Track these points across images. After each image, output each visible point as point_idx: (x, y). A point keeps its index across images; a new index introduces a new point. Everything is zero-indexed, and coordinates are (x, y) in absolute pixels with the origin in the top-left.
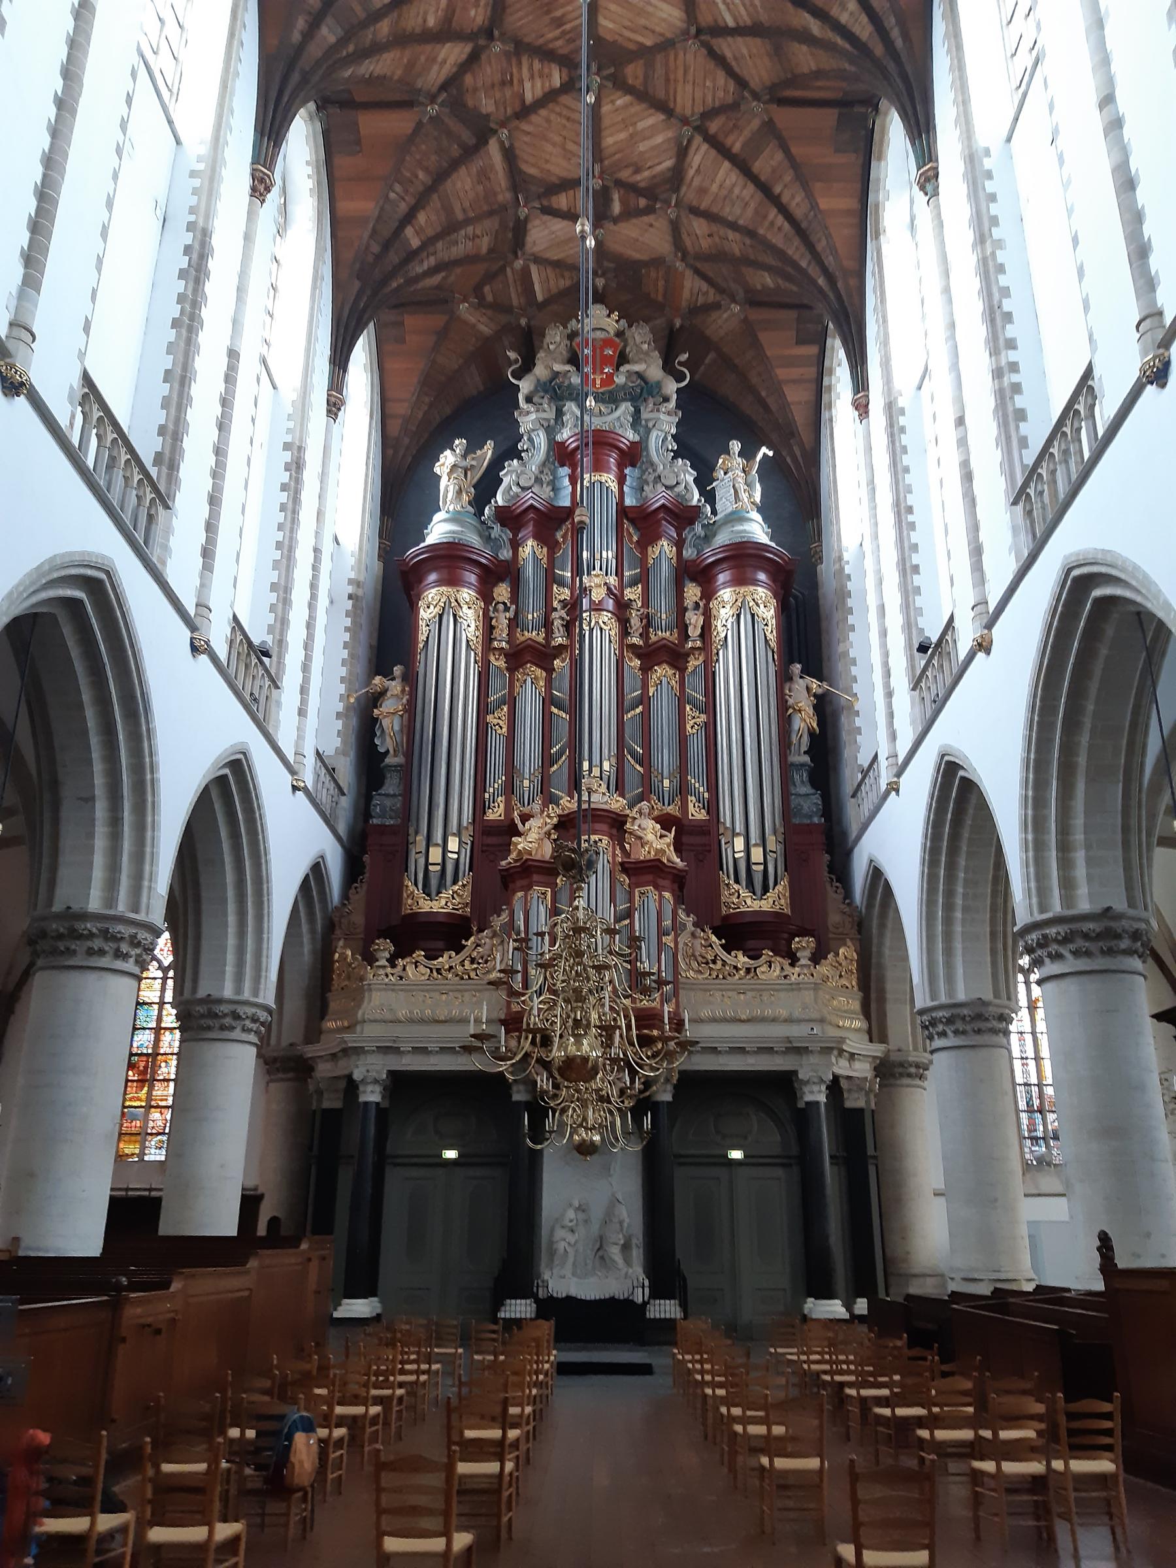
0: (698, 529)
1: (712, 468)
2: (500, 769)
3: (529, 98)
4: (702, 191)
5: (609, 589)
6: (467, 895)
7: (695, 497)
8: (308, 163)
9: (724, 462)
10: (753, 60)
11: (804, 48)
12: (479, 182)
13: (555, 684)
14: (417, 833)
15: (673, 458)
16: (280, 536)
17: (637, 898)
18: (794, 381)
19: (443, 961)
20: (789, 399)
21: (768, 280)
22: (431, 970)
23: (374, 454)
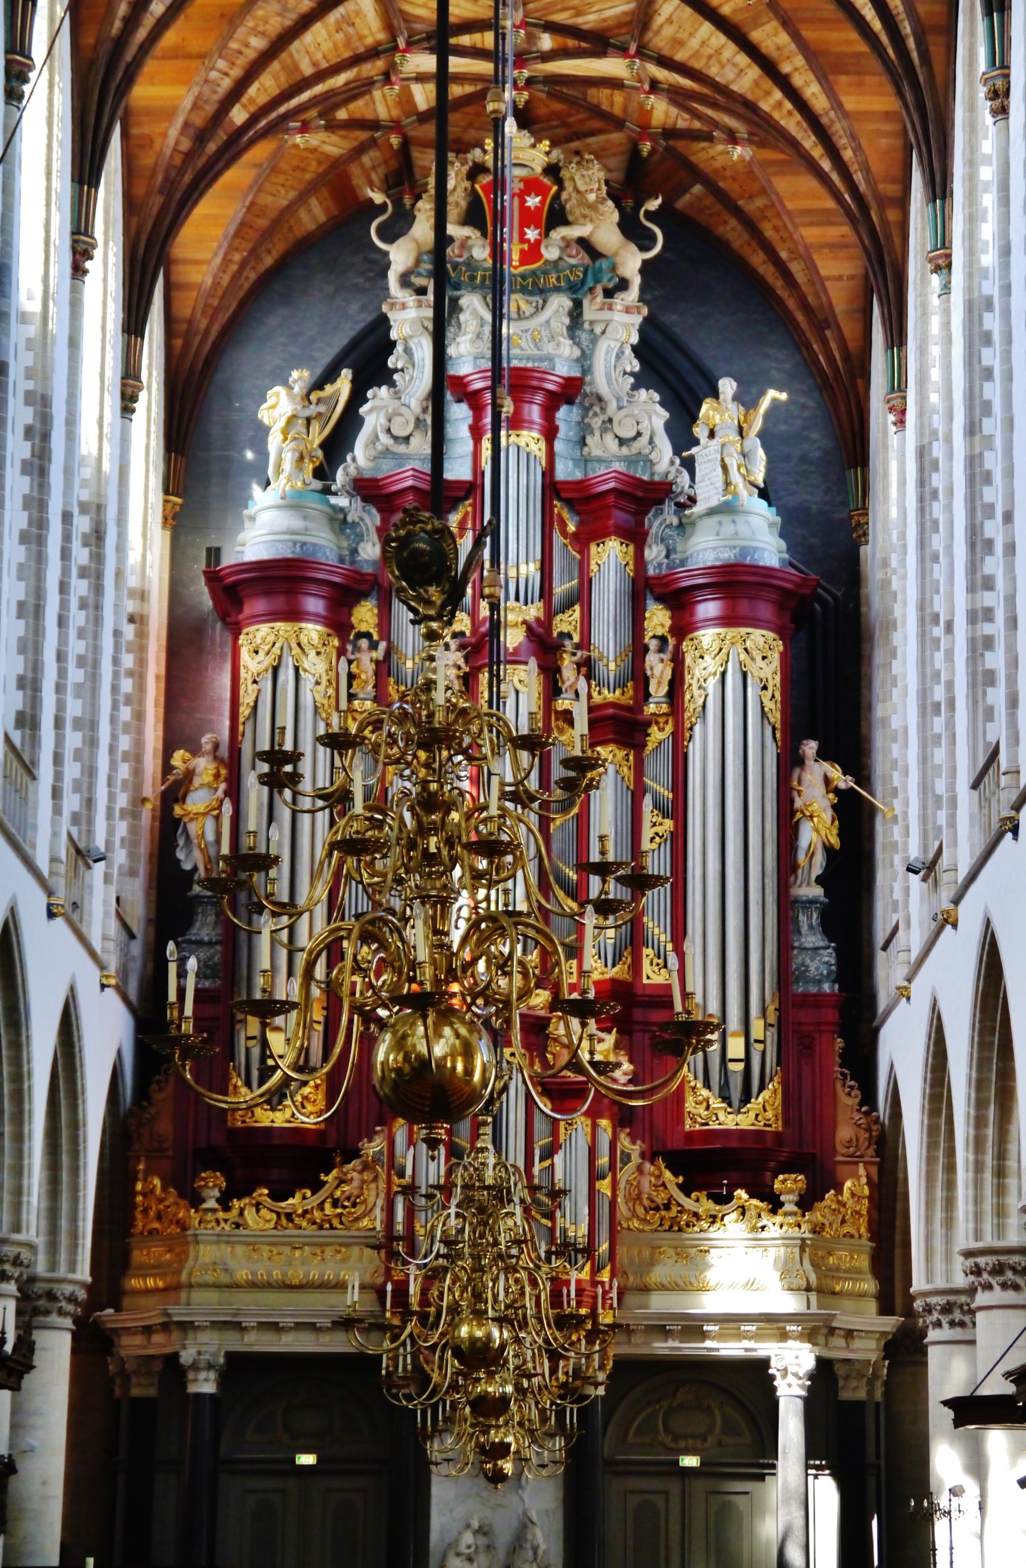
0: (669, 508)
1: (694, 418)
7: (664, 457)
15: (635, 387)
17: (562, 1130)
18: (831, 246)
19: (294, 1202)
20: (823, 272)
22: (278, 1214)
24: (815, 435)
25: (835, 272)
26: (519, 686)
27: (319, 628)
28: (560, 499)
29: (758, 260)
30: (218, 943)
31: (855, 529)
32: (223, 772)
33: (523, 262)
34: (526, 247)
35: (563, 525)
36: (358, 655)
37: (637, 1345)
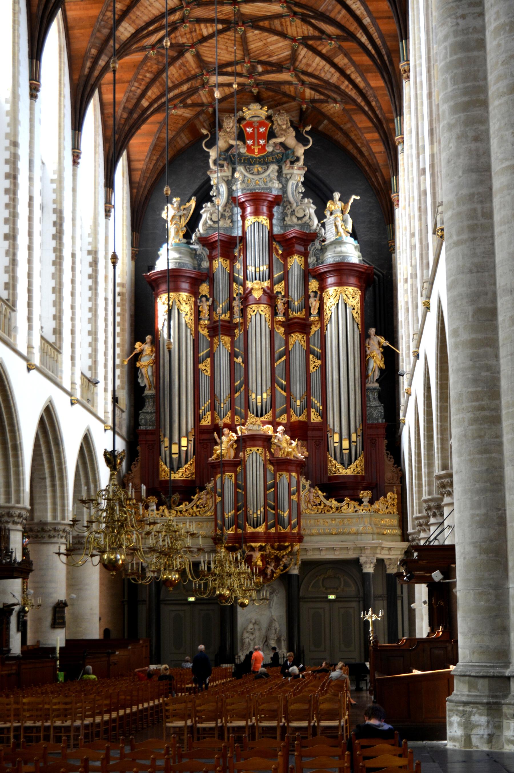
2: (207, 396)
5: (264, 291)
6: (193, 469)
13: (237, 344)
14: (165, 436)
15: (303, 198)
20: (374, 151)
22: (177, 511)
23: (127, 199)
24: (374, 213)
25: (378, 150)
26: (261, 313)
27: (187, 294)
28: (276, 241)
29: (350, 147)
30: (154, 412)
31: (390, 248)
32: (154, 349)
33: (259, 153)
34: (260, 147)
35: (277, 251)
37: (310, 556)
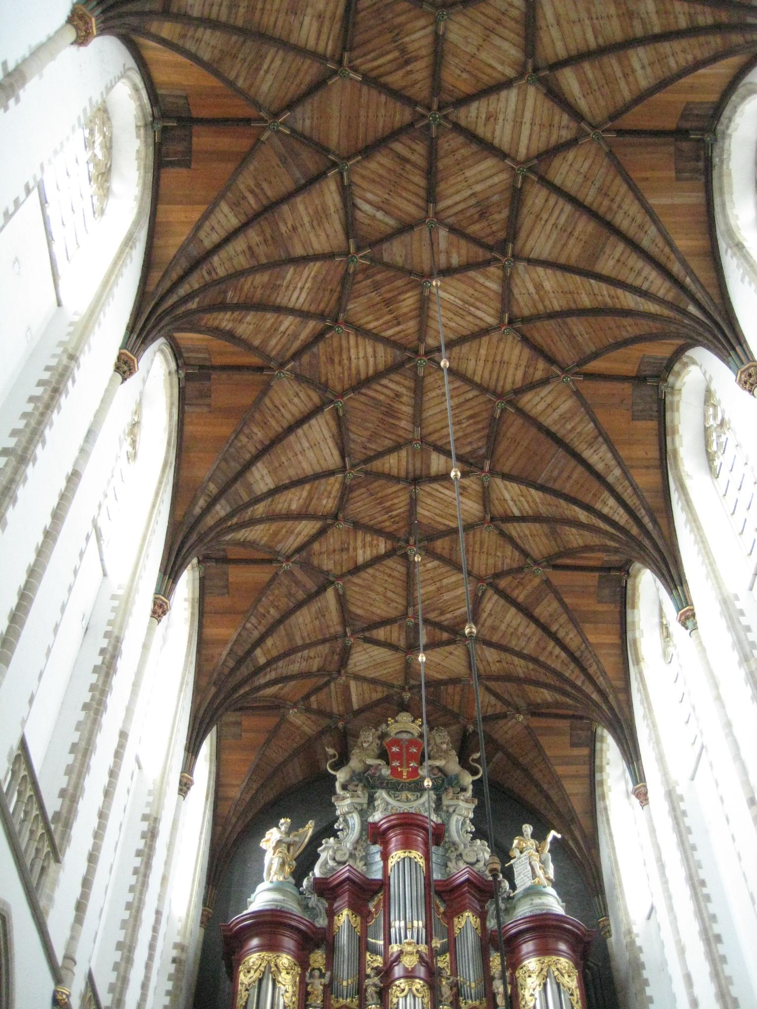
3: (360, 560)
4: (494, 629)
5: (421, 957)
8: (186, 600)
9: (519, 843)
10: (536, 540)
11: (574, 530)
12: (317, 618)
15: (473, 839)
16: (130, 897)
21: (547, 695)
25: (575, 791)
26: (415, 992)
33: (408, 778)
36: (312, 980)
